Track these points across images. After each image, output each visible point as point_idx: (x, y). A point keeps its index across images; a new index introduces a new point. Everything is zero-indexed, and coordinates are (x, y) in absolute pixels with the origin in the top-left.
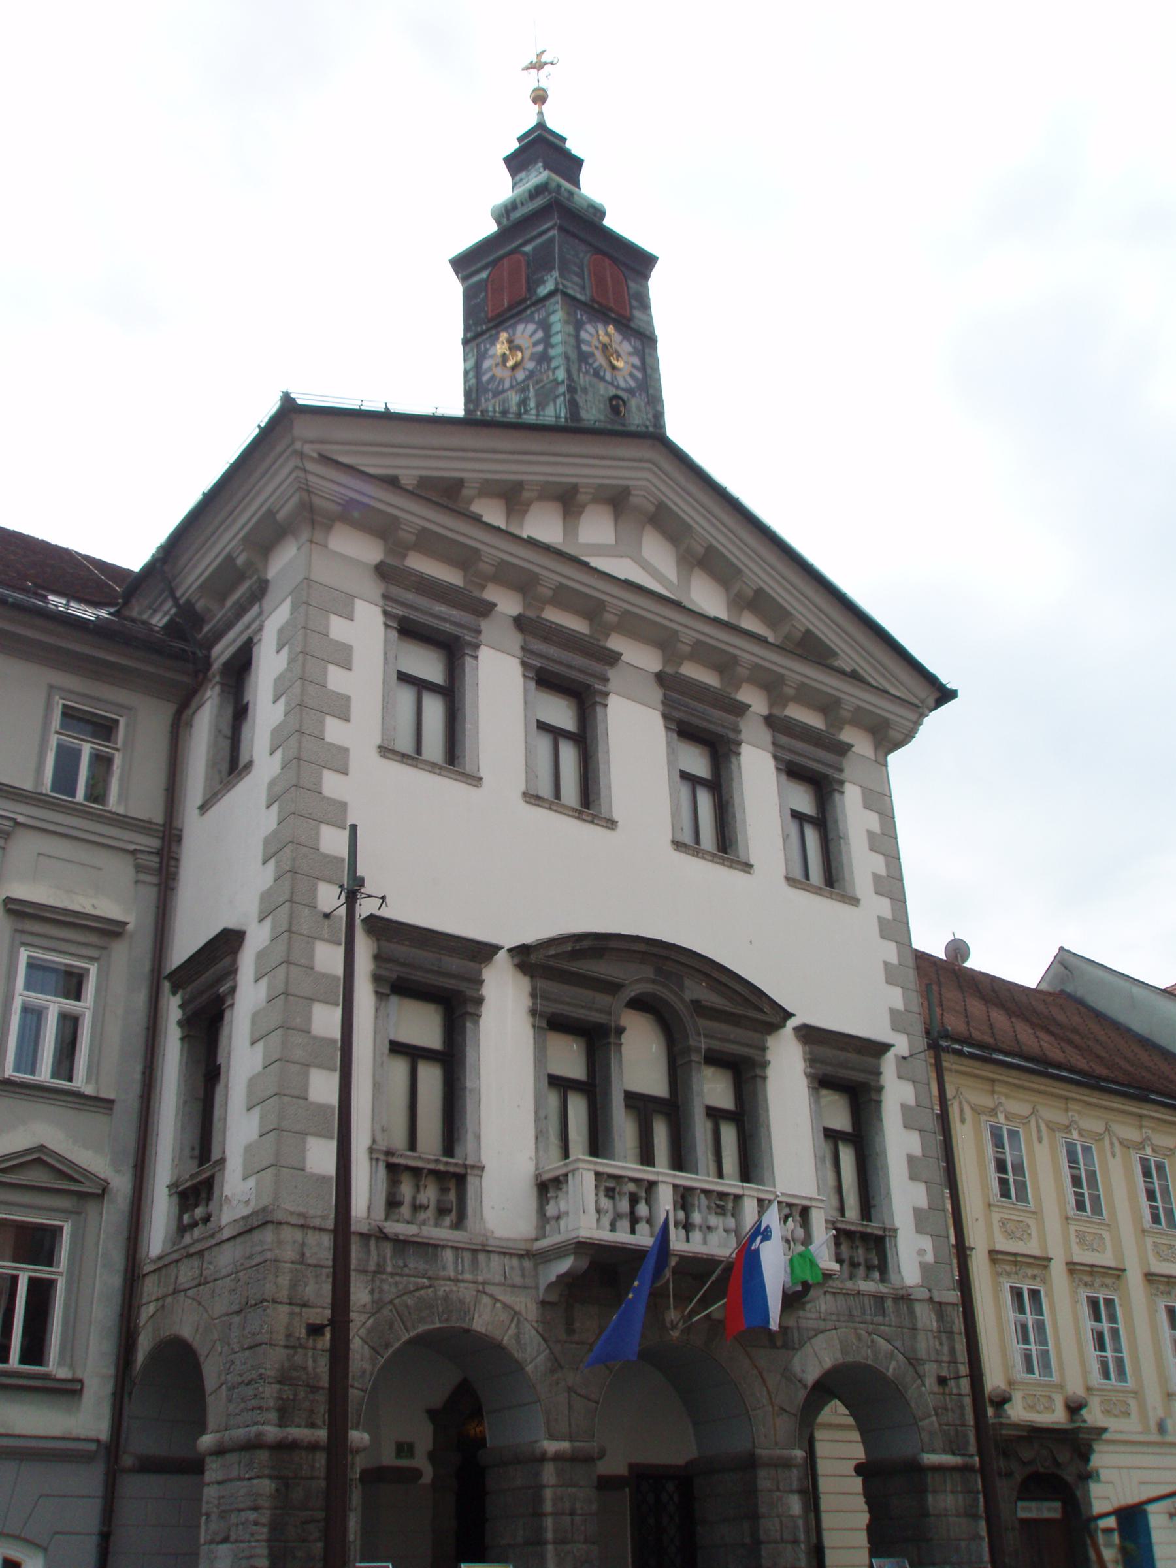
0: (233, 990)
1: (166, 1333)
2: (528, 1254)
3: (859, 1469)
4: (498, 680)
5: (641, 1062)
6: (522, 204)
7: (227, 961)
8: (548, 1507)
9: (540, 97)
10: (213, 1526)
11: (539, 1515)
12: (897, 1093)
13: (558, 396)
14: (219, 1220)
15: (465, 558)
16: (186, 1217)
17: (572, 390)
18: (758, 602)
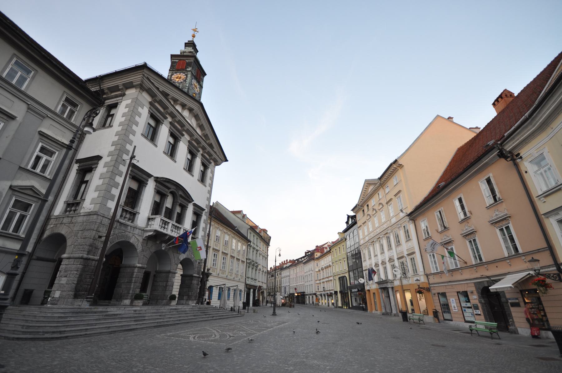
0: (96, 167)
1: (56, 231)
2: (143, 230)
3: (181, 275)
4: (164, 131)
5: (168, 203)
7: (96, 161)
8: (134, 276)
10: (61, 274)
11: (132, 277)
12: (204, 217)
15: (165, 108)
16: (68, 209)
17: (189, 89)
18: (206, 136)
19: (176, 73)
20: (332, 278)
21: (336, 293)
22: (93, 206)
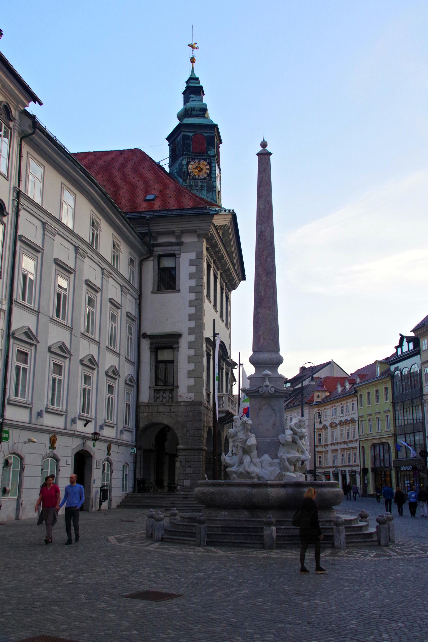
0: (178, 348)
6: (197, 110)
9: (193, 60)
13: (214, 191)
14: (178, 399)
19: (193, 159)
20: (357, 445)
21: (365, 471)
22: (192, 395)
